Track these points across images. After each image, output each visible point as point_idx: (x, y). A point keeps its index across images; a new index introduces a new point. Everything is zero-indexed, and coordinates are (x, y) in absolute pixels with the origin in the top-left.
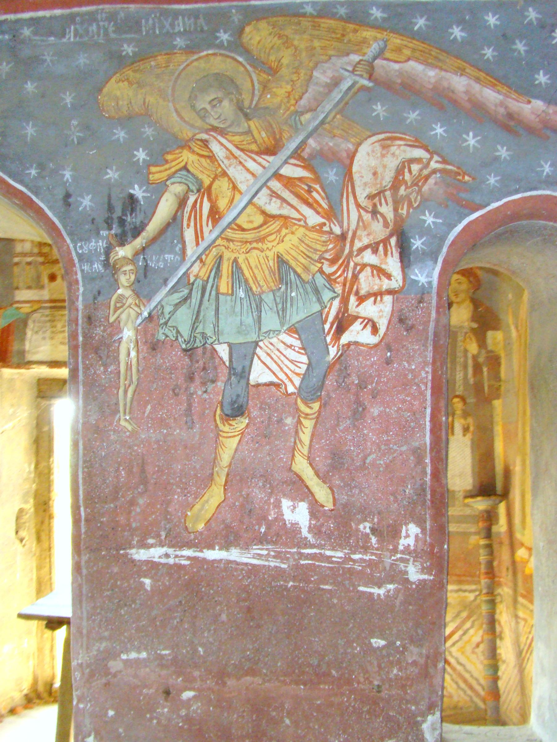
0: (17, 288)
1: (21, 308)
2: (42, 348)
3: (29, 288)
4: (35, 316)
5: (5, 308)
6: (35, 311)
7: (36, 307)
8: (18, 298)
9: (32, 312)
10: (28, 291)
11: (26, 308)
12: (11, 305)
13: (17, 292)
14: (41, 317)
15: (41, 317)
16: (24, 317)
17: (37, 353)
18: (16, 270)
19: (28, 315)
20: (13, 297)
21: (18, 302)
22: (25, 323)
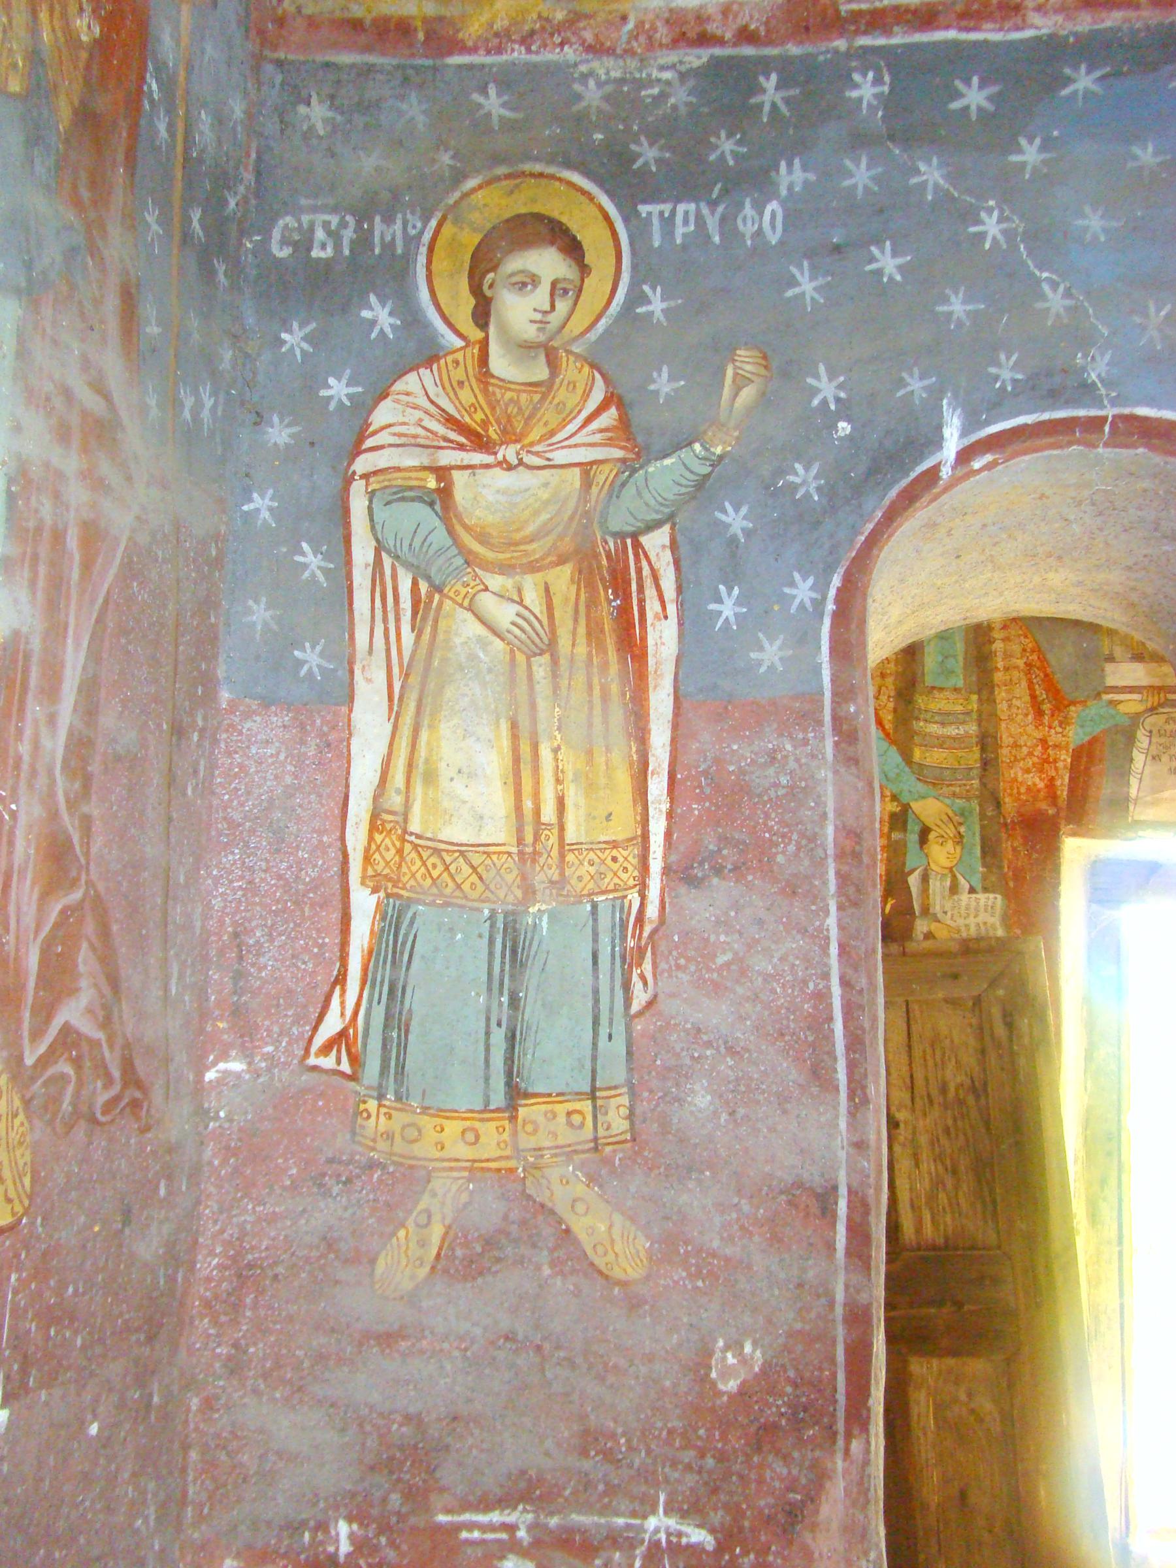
0: (1111, 659)
1: (1121, 702)
8: (1110, 681)
9: (1146, 711)
11: (1132, 704)
12: (1098, 695)
13: (1109, 667)
15: (1167, 722)
16: (1126, 721)
19: (1136, 719)
20: (1103, 677)
22: (1131, 739)
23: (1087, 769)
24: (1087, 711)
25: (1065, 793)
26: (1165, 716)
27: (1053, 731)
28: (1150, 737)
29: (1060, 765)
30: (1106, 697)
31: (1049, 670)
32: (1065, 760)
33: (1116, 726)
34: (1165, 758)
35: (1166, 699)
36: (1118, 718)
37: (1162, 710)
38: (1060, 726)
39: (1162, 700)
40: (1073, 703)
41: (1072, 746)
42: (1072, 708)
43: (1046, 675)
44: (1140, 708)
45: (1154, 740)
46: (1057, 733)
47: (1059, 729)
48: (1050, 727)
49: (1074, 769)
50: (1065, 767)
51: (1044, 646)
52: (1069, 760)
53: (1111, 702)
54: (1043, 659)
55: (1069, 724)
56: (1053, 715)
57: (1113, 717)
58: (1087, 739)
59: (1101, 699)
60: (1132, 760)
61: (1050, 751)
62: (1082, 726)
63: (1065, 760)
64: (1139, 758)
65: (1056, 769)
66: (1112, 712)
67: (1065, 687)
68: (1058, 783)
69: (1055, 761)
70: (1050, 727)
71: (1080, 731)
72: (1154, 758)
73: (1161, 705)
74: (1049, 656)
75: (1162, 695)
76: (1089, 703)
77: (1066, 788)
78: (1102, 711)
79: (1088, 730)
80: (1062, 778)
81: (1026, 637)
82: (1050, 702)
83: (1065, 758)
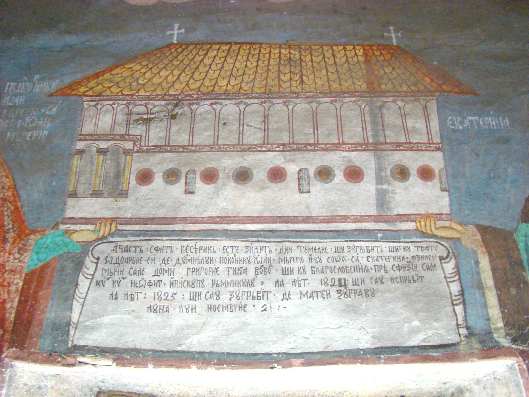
0: (74, 195)
1: (75, 231)
2: (106, 319)
3: (96, 194)
4: (103, 249)
5: (42, 232)
6: (102, 239)
7: (104, 230)
8: (69, 213)
9: (98, 239)
10: (93, 200)
12: (56, 225)
13: (71, 202)
14: (115, 250)
15: (115, 250)
16: (78, 249)
17: (91, 329)
18: (76, 161)
20: (63, 210)
21: (72, 221)
22: (79, 264)
23: (36, 292)
24: (45, 239)
25: (13, 316)
26: (113, 245)
27: (12, 256)
28: (97, 263)
29: (13, 288)
30: (62, 227)
31: (19, 204)
32: (17, 284)
33: (69, 252)
34: (108, 284)
35: (117, 230)
36: (71, 245)
37: (111, 239)
38: (19, 253)
39: (113, 229)
40: (33, 232)
41: (25, 271)
42: (32, 236)
43: (16, 208)
44: (92, 237)
45: (100, 266)
46: (15, 259)
47: (17, 256)
48: (10, 254)
49: (24, 293)
50: (17, 290)
51: (20, 184)
52: (21, 284)
53: (67, 231)
54: (16, 195)
55: (26, 251)
56: (14, 242)
57: (66, 245)
58: (40, 264)
59: (58, 229)
60: (77, 285)
61: (6, 276)
62: (37, 253)
63: (17, 284)
64: (84, 283)
65: (9, 292)
66: (67, 240)
67: (29, 217)
68: (8, 306)
69: (9, 284)
70: (10, 254)
71: (35, 257)
72: (98, 283)
73: (111, 235)
74: (21, 192)
75: (113, 226)
76: (47, 232)
77: (14, 311)
78: (58, 239)
79: (42, 256)
80: (13, 301)
81: (7, 177)
82: (14, 231)
83: (19, 282)
